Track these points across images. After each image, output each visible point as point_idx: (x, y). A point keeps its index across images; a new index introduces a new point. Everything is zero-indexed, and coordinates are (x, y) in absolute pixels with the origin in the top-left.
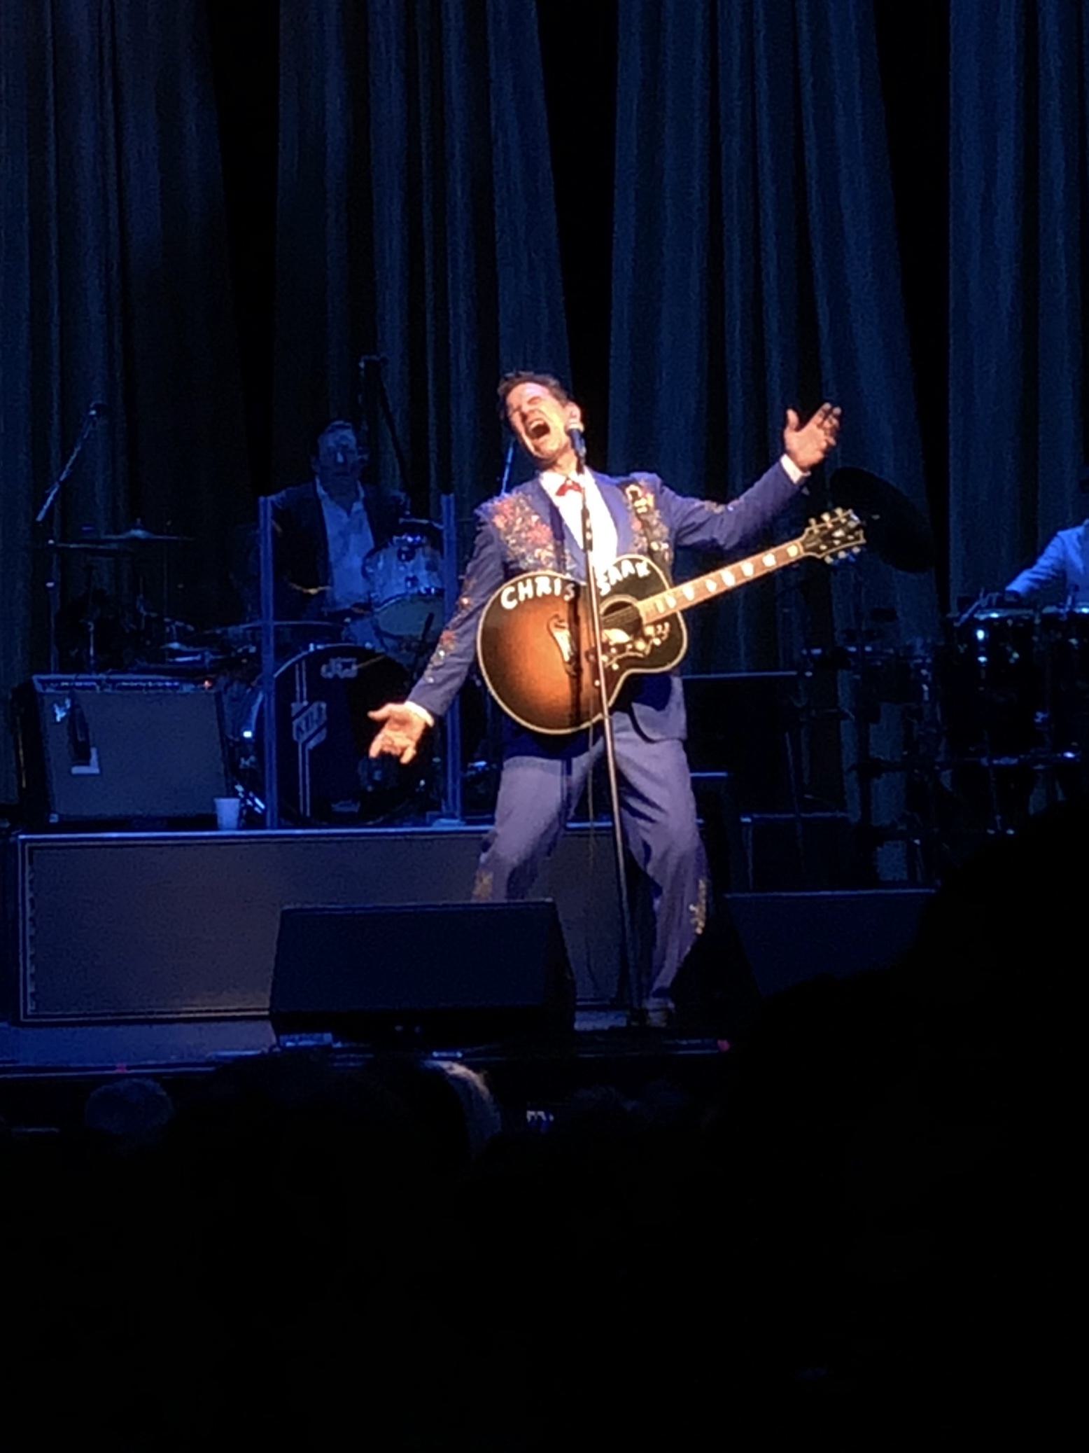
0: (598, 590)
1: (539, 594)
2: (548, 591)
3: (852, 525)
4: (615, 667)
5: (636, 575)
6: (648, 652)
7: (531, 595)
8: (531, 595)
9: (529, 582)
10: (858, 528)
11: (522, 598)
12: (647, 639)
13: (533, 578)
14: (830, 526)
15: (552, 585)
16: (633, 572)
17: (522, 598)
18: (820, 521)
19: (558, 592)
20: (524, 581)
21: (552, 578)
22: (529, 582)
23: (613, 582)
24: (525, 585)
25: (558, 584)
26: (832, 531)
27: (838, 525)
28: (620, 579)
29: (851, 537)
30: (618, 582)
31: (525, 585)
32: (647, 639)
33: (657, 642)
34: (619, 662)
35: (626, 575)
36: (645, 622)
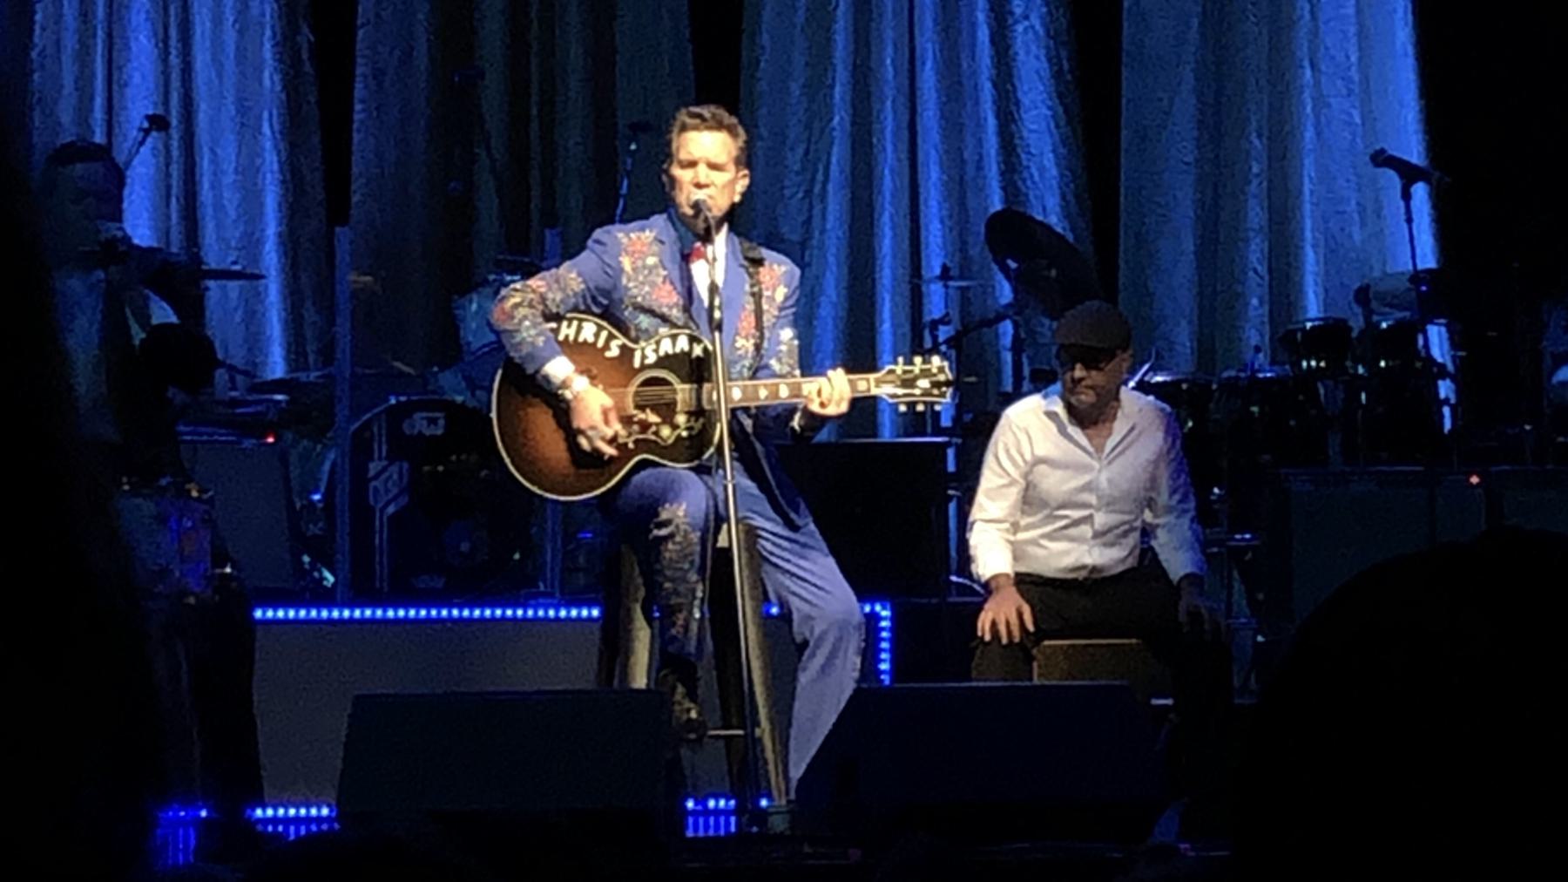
0: (644, 357)
1: (581, 339)
2: (591, 339)
3: (942, 378)
4: (631, 446)
5: (689, 353)
6: (670, 441)
7: (571, 338)
8: (571, 338)
9: (575, 323)
10: (947, 383)
11: (561, 338)
12: (675, 427)
13: (581, 320)
14: (917, 370)
15: (597, 335)
16: (686, 348)
17: (561, 338)
18: (909, 362)
19: (600, 344)
20: (570, 320)
21: (600, 328)
22: (575, 323)
23: (662, 353)
24: (569, 326)
25: (604, 334)
26: (916, 378)
27: (925, 373)
28: (670, 352)
29: (936, 392)
30: (667, 356)
31: (569, 326)
32: (675, 427)
33: (685, 434)
34: (636, 442)
35: (678, 350)
36: (679, 407)
